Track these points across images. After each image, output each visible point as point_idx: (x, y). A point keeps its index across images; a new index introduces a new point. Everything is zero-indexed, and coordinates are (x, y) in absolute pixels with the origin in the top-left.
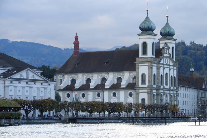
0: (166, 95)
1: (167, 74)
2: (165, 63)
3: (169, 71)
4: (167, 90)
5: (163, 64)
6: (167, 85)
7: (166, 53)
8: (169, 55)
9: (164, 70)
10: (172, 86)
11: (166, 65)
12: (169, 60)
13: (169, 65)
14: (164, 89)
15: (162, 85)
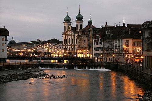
0: (69, 48)
1: (69, 38)
2: (68, 34)
3: (71, 36)
4: (70, 45)
5: (68, 34)
6: (69, 43)
7: (70, 29)
8: (71, 30)
9: (68, 37)
10: (72, 43)
11: (69, 34)
12: (71, 32)
13: (71, 34)
14: (68, 45)
15: (67, 43)
